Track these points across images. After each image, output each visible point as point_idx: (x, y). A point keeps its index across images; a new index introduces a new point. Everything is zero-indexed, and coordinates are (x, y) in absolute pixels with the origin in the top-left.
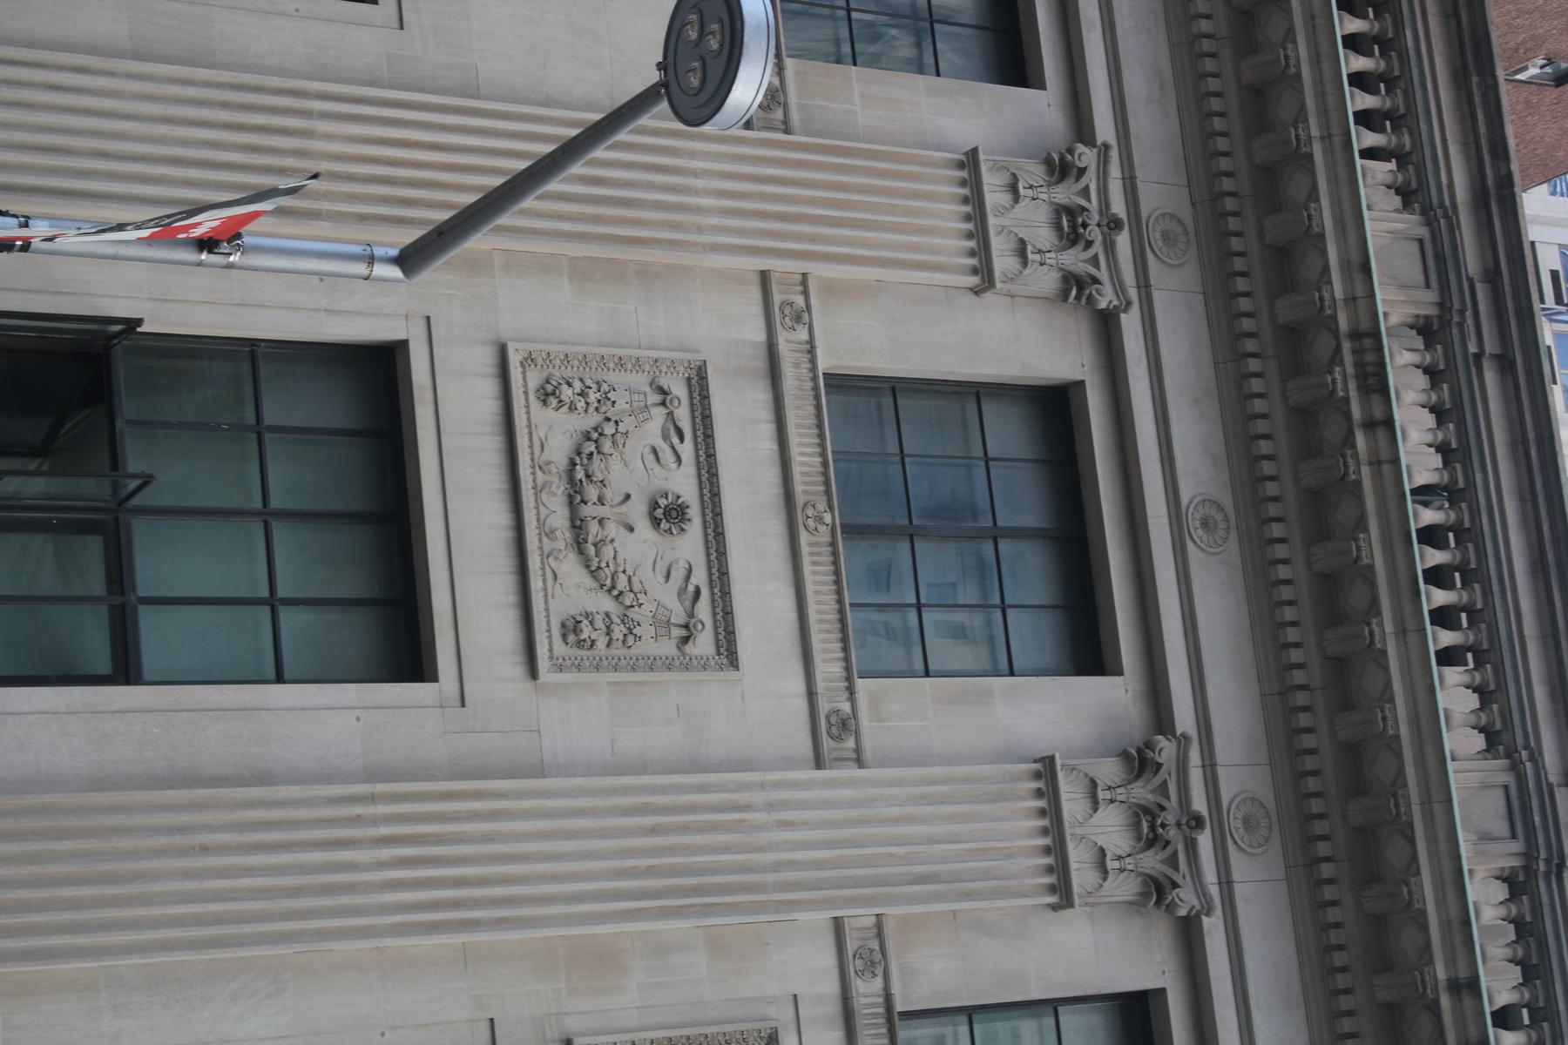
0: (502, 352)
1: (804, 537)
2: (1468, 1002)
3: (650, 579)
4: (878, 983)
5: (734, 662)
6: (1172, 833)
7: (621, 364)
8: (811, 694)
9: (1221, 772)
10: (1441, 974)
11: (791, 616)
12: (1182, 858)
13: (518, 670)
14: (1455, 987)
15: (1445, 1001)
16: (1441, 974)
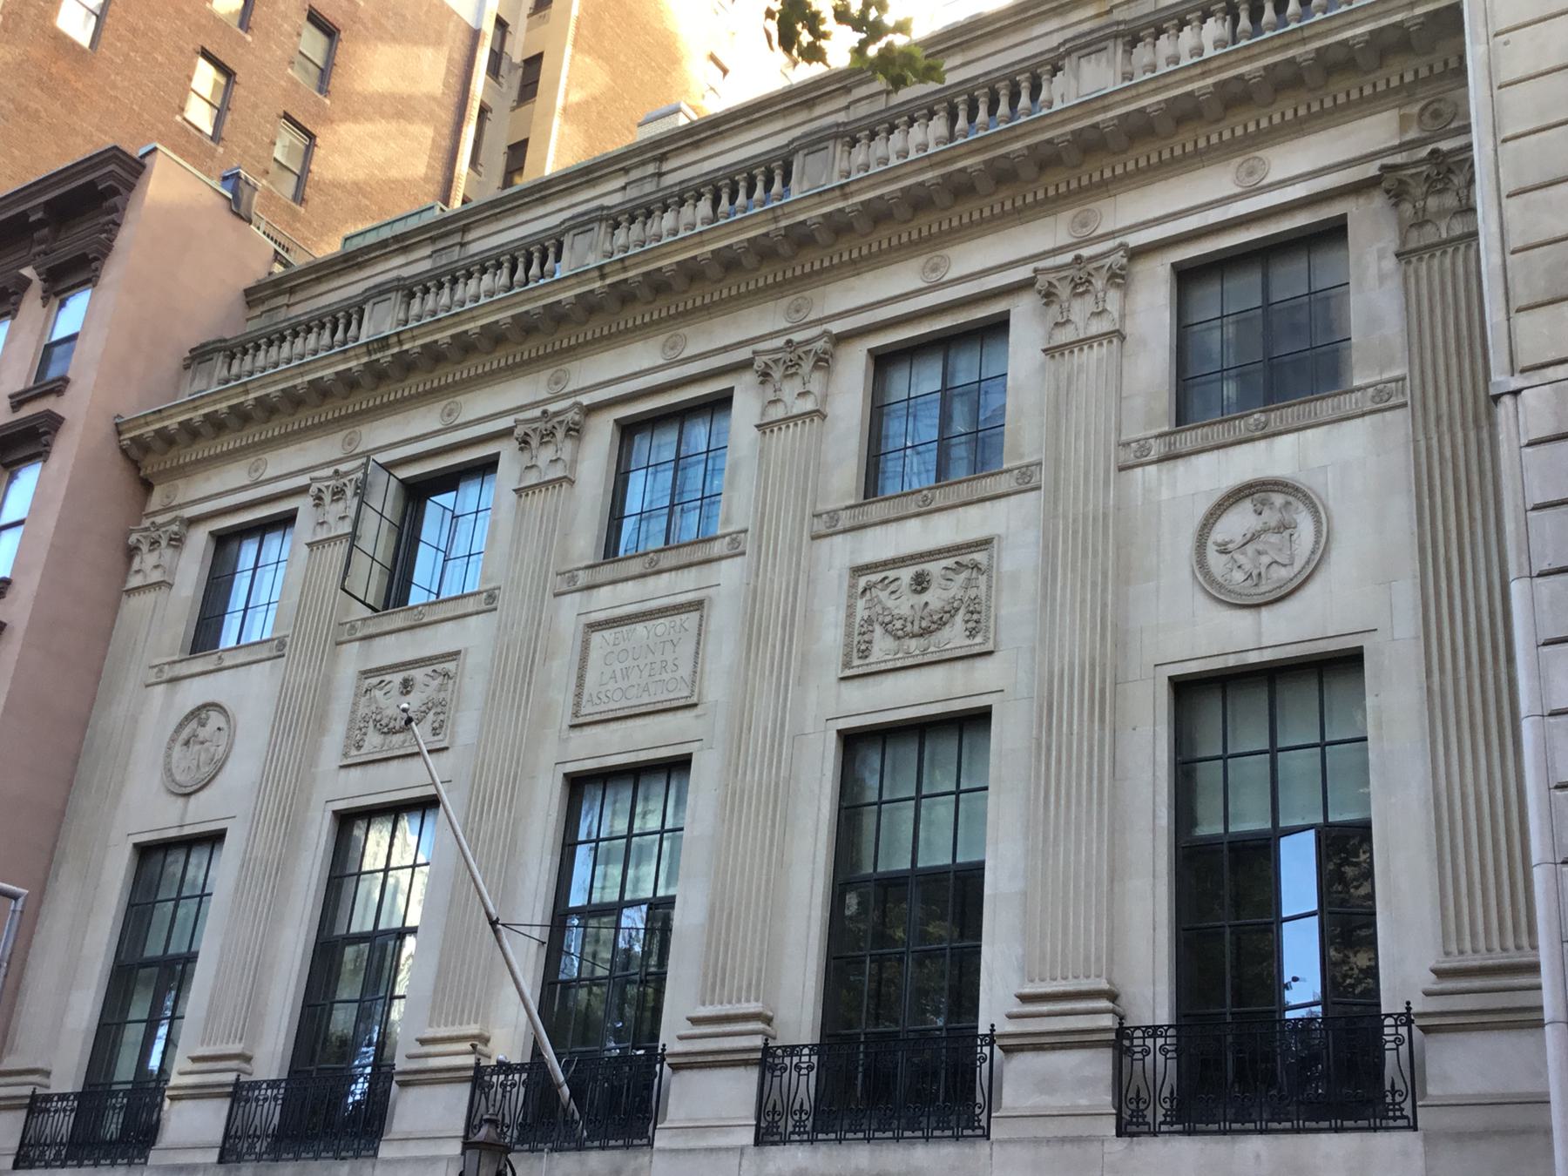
0: (342, 767)
1: (425, 620)
2: (607, 270)
3: (424, 696)
4: (581, 573)
5: (458, 653)
6: (549, 426)
7: (353, 712)
8: (478, 613)
9: (777, 328)
10: (598, 284)
11: (450, 624)
12: (1095, 265)
13: (445, 754)
14: (603, 277)
15: (608, 281)
16: (598, 284)
